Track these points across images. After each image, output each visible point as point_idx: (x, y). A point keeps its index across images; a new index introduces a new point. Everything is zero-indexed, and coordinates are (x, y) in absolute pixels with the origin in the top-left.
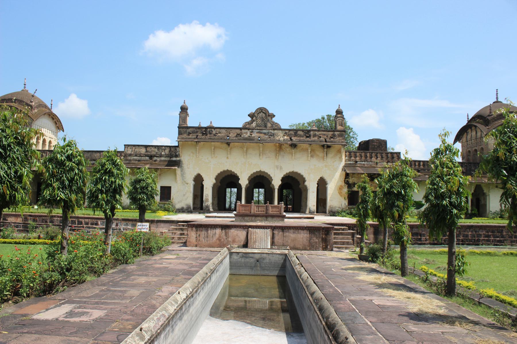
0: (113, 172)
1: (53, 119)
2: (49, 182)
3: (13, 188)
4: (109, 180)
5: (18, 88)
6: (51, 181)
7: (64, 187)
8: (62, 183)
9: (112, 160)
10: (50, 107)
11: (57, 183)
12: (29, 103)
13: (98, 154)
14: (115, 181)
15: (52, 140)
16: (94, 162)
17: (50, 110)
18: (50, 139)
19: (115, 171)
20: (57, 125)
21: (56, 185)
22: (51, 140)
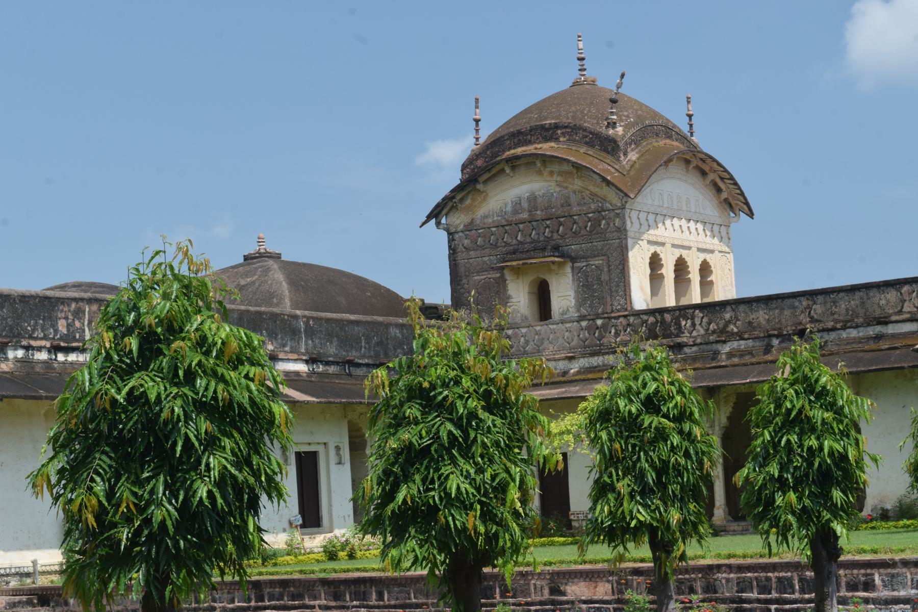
0: (808, 419)
1: (704, 174)
2: (606, 479)
3: (488, 516)
4: (801, 446)
6: (610, 476)
7: (646, 491)
8: (640, 477)
9: (806, 378)
10: (685, 129)
11: (626, 481)
12: (603, 130)
13: (892, 295)
14: (821, 448)
16: (879, 329)
18: (702, 256)
19: (818, 415)
20: (724, 195)
21: (623, 486)
22: (708, 257)
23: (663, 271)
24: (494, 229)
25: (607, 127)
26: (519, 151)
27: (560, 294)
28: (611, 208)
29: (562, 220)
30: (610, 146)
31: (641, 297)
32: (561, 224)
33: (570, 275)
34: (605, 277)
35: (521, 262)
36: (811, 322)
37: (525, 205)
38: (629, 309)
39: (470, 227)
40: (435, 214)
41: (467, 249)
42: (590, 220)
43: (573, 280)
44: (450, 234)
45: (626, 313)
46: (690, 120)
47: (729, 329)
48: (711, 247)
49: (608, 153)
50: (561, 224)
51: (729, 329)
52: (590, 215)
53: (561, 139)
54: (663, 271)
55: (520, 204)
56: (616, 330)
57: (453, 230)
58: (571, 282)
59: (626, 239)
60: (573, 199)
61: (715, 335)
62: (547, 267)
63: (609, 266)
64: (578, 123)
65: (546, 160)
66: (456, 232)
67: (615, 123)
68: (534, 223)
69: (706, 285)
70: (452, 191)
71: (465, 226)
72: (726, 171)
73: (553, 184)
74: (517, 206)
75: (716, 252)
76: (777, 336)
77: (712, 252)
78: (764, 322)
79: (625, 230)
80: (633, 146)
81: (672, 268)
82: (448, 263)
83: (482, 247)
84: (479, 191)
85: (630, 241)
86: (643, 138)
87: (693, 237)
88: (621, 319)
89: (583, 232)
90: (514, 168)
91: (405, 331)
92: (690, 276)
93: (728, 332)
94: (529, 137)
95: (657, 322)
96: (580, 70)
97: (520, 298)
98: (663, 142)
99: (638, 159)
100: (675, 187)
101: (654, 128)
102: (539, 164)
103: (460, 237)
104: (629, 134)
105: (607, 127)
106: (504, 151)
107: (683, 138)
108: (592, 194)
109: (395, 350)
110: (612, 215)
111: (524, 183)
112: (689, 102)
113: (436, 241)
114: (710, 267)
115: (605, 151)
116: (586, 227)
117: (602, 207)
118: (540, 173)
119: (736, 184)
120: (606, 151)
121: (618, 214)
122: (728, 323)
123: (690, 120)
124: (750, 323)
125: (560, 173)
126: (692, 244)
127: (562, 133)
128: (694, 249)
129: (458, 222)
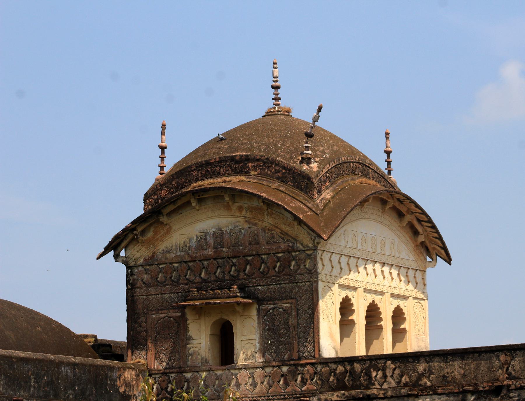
1: (400, 215)
5: (251, 108)
10: (383, 166)
12: (297, 165)
15: (407, 306)
17: (382, 178)
18: (396, 303)
20: (421, 238)
22: (402, 303)
23: (354, 317)
24: (176, 265)
25: (301, 162)
26: (207, 183)
27: (244, 338)
28: (302, 248)
29: (249, 258)
30: (303, 183)
31: (329, 343)
32: (248, 263)
33: (256, 318)
34: (292, 321)
35: (204, 302)
36: (508, 379)
37: (211, 241)
38: (317, 356)
39: (150, 261)
40: (114, 245)
41: (147, 285)
42: (279, 260)
43: (259, 323)
44: (129, 268)
45: (314, 361)
46: (388, 157)
47: (422, 383)
48: (406, 293)
49: (302, 190)
50: (248, 263)
51: (422, 383)
52: (280, 255)
53: (252, 173)
54: (354, 317)
55: (205, 239)
56: (302, 378)
57: (132, 264)
58: (256, 325)
59: (317, 282)
60: (262, 235)
61: (407, 389)
62: (232, 308)
63: (298, 310)
64: (270, 156)
65: (236, 194)
66: (136, 266)
67: (310, 159)
68: (220, 261)
69: (398, 333)
70: (133, 223)
71: (145, 260)
72: (424, 213)
73: (242, 220)
74: (202, 240)
75: (411, 298)
76: (472, 393)
77: (406, 298)
78: (458, 377)
79: (316, 273)
80: (327, 184)
81: (364, 314)
82: (125, 298)
83: (163, 284)
84: (162, 223)
85: (321, 285)
86: (339, 175)
87: (386, 282)
88: (308, 367)
89: (271, 273)
90: (200, 201)
91: (77, 370)
92: (382, 323)
93: (421, 385)
94: (218, 169)
95: (346, 371)
96: (274, 99)
97: (201, 340)
98: (359, 180)
99: (332, 197)
100: (371, 230)
101: (351, 165)
102: (227, 199)
103: (139, 271)
104: (324, 171)
105: (301, 162)
106: (190, 182)
107: (380, 176)
108: (283, 232)
109: (66, 390)
110: (303, 256)
111: (211, 218)
112: (387, 138)
113: (115, 274)
114: (404, 314)
115: (297, 188)
116: (274, 268)
117: (292, 247)
118: (228, 208)
119: (434, 227)
120: (298, 187)
121: (309, 256)
122: (421, 376)
123: (388, 157)
124: (444, 377)
125: (250, 209)
126: (385, 289)
127: (254, 166)
128: (387, 295)
129: (138, 255)
